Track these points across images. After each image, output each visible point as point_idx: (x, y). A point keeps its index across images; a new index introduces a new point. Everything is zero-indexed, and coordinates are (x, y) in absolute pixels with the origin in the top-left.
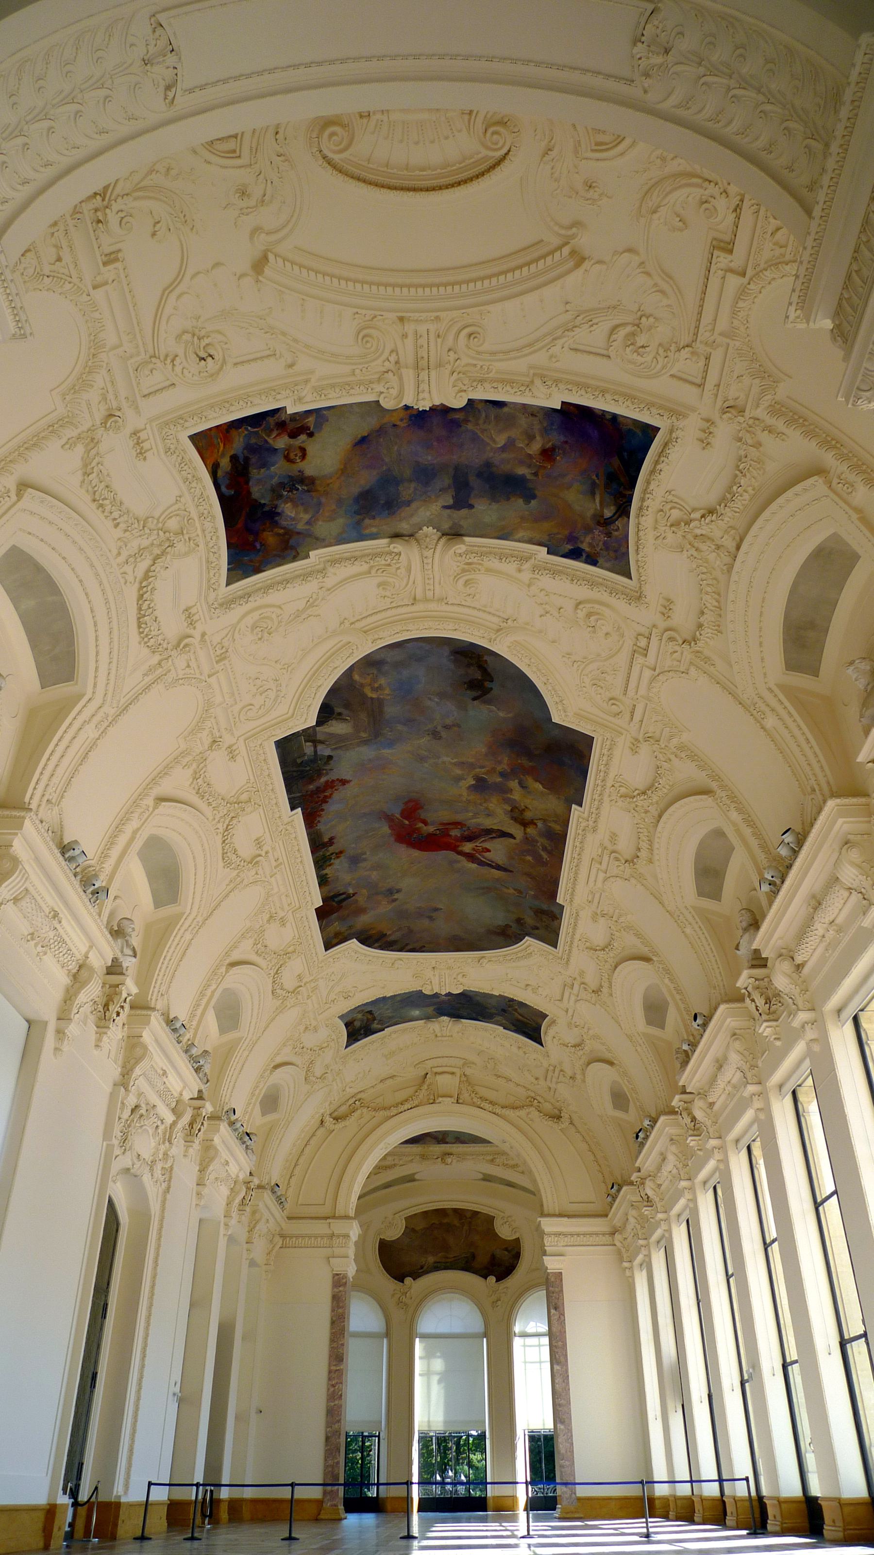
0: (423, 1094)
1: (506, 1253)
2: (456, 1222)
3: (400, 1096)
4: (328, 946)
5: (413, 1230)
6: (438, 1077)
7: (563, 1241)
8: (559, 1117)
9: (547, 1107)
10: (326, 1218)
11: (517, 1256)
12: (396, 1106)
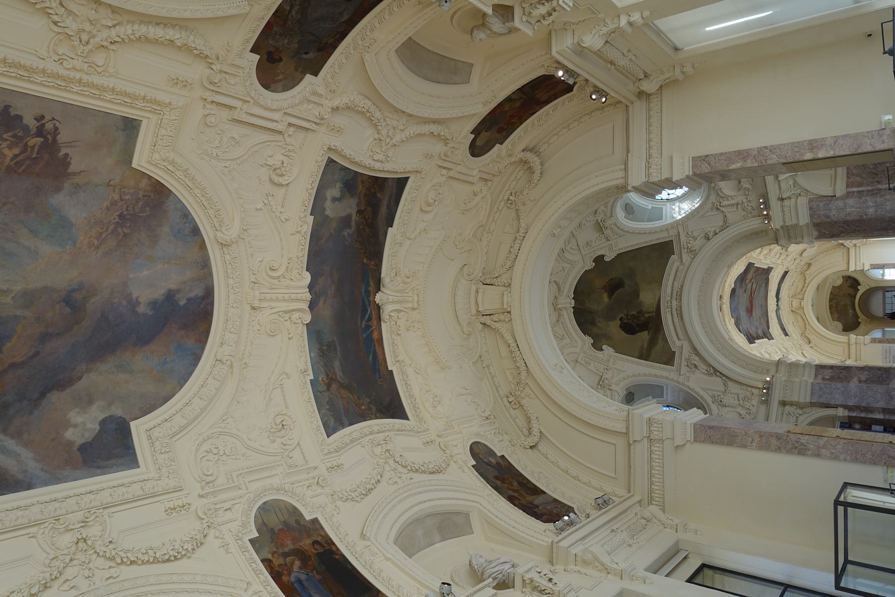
0: (800, 312)
1: (848, 282)
2: (835, 301)
3: (800, 319)
4: (773, 339)
5: (838, 318)
6: (794, 306)
7: (858, 263)
8: (810, 264)
9: (805, 268)
10: (849, 345)
11: (849, 277)
12: (804, 321)
